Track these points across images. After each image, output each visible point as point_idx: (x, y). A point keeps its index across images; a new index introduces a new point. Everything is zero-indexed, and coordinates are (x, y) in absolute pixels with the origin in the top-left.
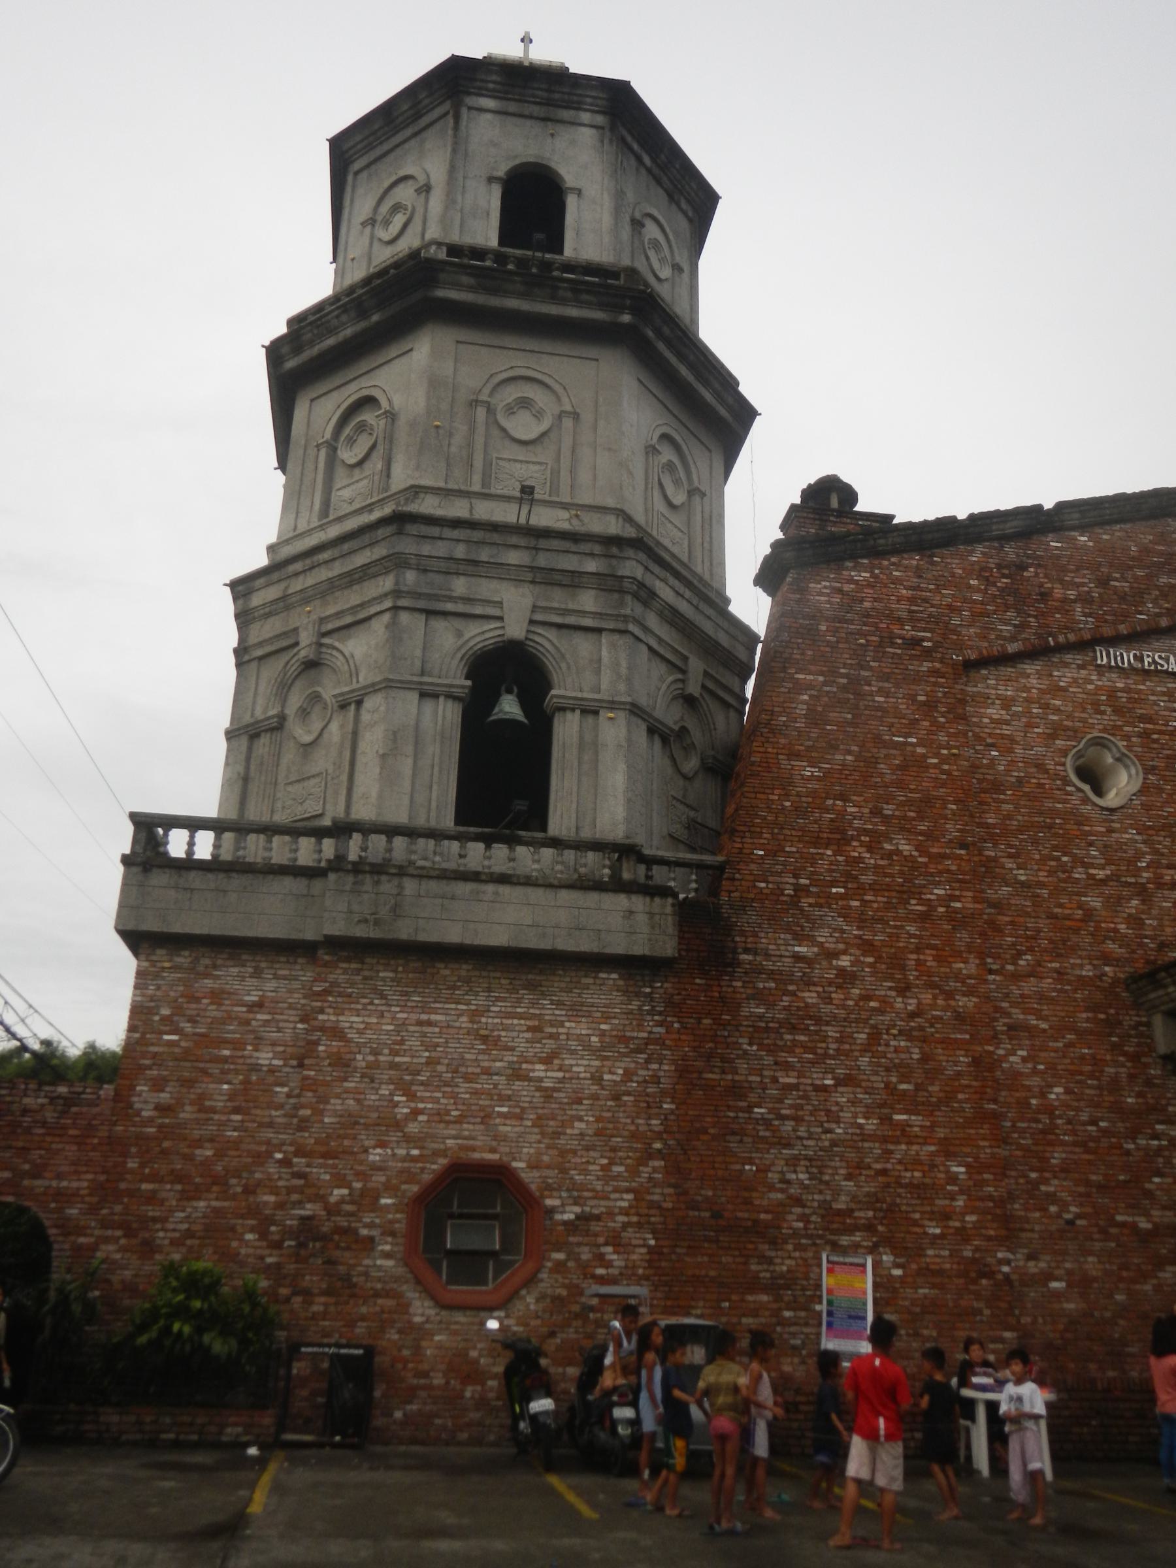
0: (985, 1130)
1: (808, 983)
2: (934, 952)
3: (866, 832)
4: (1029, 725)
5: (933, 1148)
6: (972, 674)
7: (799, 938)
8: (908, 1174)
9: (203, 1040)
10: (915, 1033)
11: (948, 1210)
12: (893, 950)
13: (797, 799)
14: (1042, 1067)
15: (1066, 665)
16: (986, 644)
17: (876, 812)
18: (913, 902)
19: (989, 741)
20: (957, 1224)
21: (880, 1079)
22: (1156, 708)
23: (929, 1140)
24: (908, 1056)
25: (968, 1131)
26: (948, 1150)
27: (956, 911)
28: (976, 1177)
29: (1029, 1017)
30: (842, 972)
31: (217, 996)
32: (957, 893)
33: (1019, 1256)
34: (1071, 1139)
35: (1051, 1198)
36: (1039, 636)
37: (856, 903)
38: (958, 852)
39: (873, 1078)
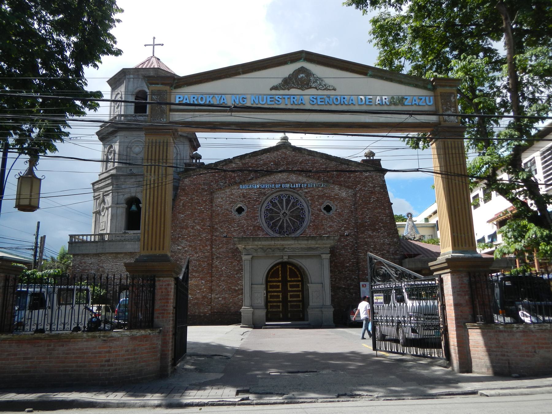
0: (209, 275)
1: (179, 253)
4: (226, 202)
7: (178, 245)
9: (83, 270)
15: (235, 189)
17: (194, 222)
26: (202, 279)
30: (186, 250)
31: (85, 263)
35: (221, 285)
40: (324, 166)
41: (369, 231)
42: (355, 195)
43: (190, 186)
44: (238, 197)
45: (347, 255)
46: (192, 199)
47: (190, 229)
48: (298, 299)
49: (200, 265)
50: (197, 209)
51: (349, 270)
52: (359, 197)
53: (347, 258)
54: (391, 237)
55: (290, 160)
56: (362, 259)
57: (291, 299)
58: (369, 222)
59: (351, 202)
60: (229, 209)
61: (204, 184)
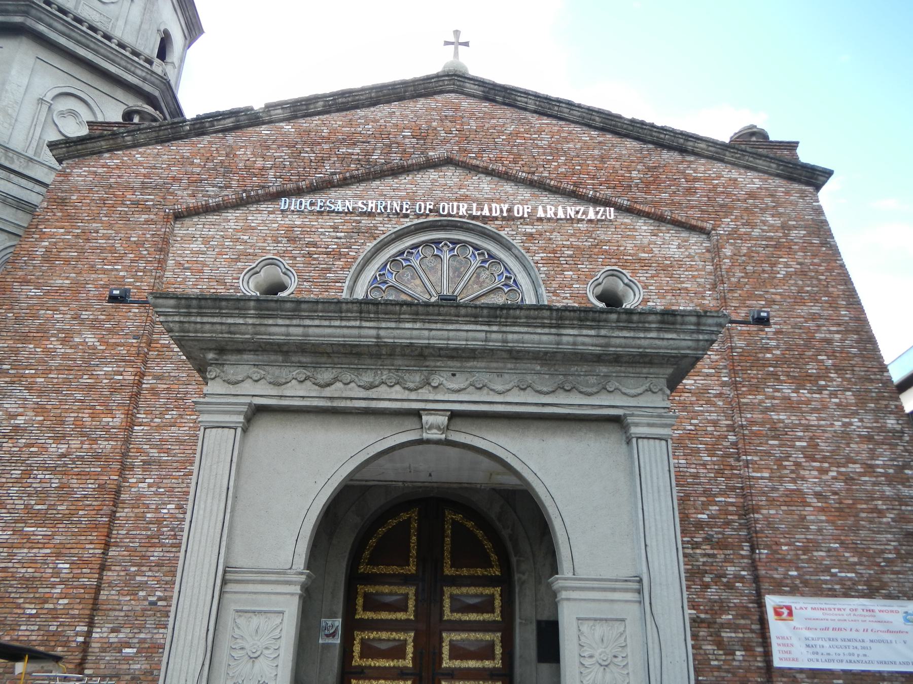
2: (91, 411)
3: (60, 331)
4: (220, 254)
5: (48, 551)
6: (187, 222)
8: (23, 570)
10: (58, 469)
11: (47, 596)
12: (59, 411)
13: (18, 311)
14: (162, 490)
15: (260, 212)
16: (194, 201)
17: (76, 317)
18: (85, 377)
19: (186, 265)
20: (51, 606)
21: (22, 502)
22: (321, 237)
23: (46, 545)
24: (48, 485)
25: (79, 538)
27: (119, 381)
28: (76, 571)
29: (162, 455)
30: (16, 428)
32: (122, 369)
33: (104, 629)
34: (171, 541)
35: (142, 586)
36: (236, 193)
37: (42, 380)
38: (130, 341)
39: (16, 502)
40: (596, 152)
41: (781, 382)
42: (716, 251)
43: (90, 191)
44: (269, 240)
45: (696, 476)
46: (86, 236)
47: (54, 344)
48: (488, 664)
49: (64, 492)
50: (96, 272)
51: (708, 540)
52: (731, 258)
53: (700, 489)
54: (874, 410)
55: (473, 125)
56: (764, 493)
57: (457, 664)
58: (777, 347)
59: (699, 276)
60: (228, 280)
61: (144, 186)
